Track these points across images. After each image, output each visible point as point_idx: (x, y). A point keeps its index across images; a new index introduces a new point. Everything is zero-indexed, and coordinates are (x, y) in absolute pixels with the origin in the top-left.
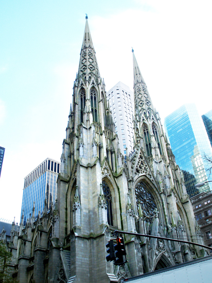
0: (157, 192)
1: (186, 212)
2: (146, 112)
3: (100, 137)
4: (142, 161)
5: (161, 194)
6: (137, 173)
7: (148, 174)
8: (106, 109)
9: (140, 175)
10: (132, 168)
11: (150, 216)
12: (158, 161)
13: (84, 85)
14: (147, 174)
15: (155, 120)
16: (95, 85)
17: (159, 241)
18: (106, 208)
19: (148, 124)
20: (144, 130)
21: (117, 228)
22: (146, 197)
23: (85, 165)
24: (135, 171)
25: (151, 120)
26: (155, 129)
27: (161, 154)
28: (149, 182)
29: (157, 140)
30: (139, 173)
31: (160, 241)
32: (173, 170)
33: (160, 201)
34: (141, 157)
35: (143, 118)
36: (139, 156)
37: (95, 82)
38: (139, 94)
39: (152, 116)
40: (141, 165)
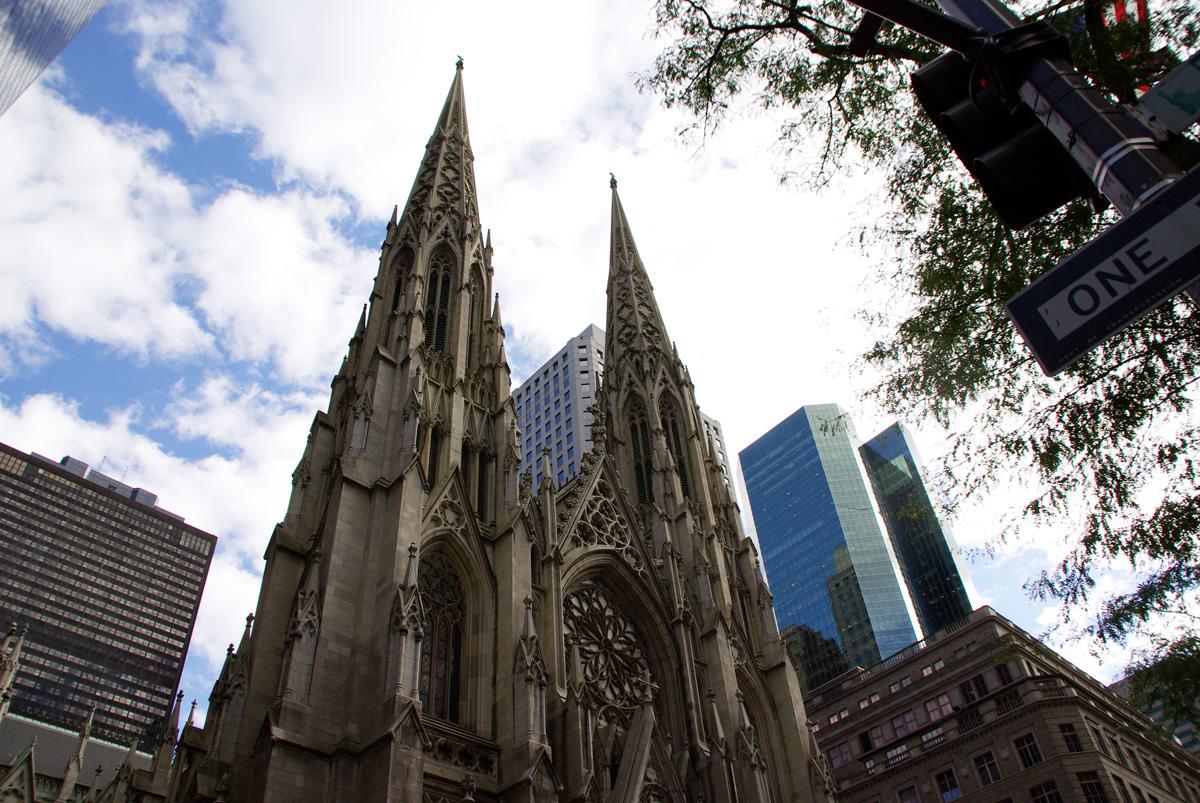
0: (658, 620)
1: (776, 701)
2: (642, 358)
3: (442, 397)
4: (605, 503)
5: (676, 628)
6: (583, 542)
7: (627, 551)
8: (485, 319)
9: (595, 547)
10: (562, 518)
11: (624, 705)
12: (673, 513)
13: (412, 240)
14: (624, 548)
15: (671, 387)
16: (452, 241)
17: (652, 798)
18: (417, 638)
19: (646, 397)
20: (633, 418)
21: (473, 729)
22: (614, 633)
23: (366, 482)
24: (572, 530)
25: (657, 385)
26: (672, 415)
27: (686, 493)
28: (629, 579)
29: (674, 451)
30: (592, 541)
31: (654, 796)
32: (731, 552)
33: (671, 651)
34: (603, 489)
35: (630, 376)
36: (595, 484)
37: (451, 231)
38: (622, 307)
39: (660, 373)
40: (603, 516)
